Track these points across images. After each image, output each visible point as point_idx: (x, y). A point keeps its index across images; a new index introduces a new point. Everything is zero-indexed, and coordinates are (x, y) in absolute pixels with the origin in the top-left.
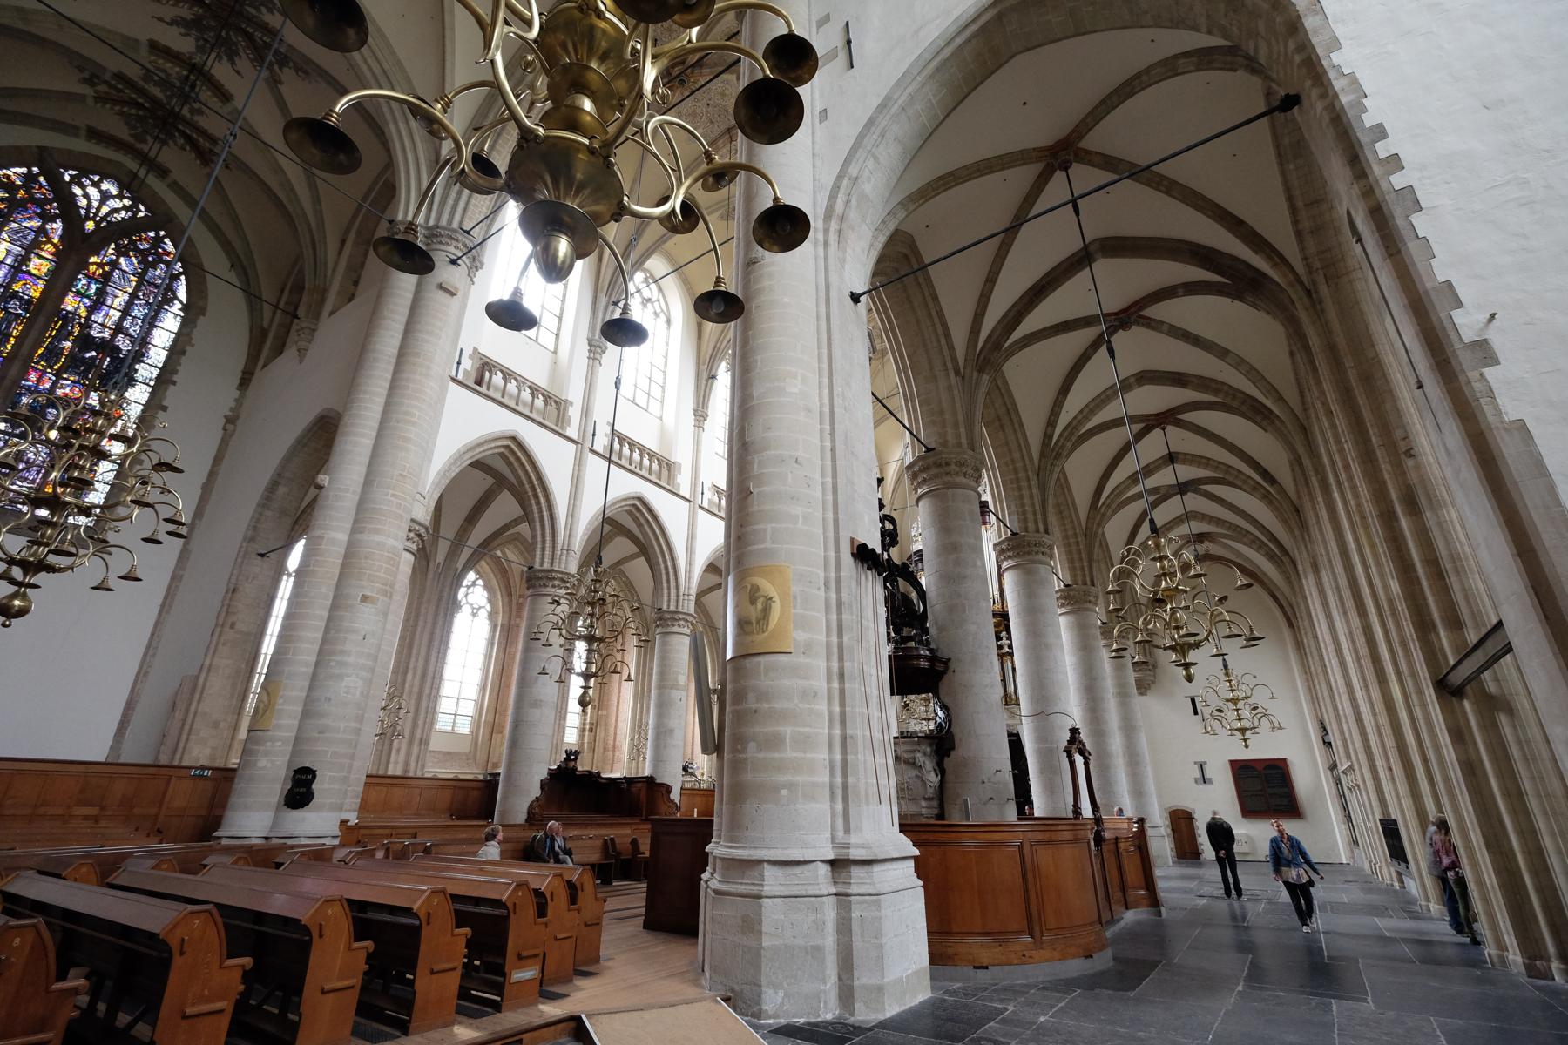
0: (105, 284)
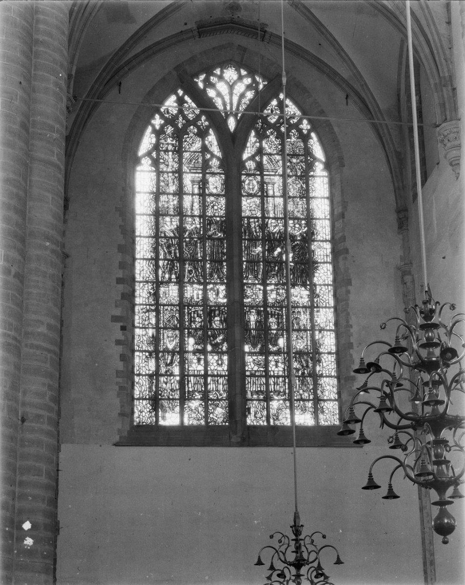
0: (262, 175)
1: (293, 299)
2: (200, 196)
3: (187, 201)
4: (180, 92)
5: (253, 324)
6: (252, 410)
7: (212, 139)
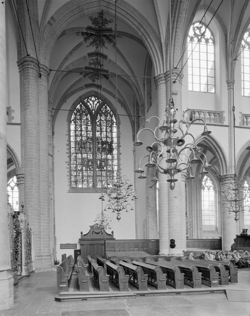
0: (101, 126)
1: (108, 158)
2: (86, 131)
3: (83, 133)
4: (81, 103)
5: (98, 164)
6: (98, 184)
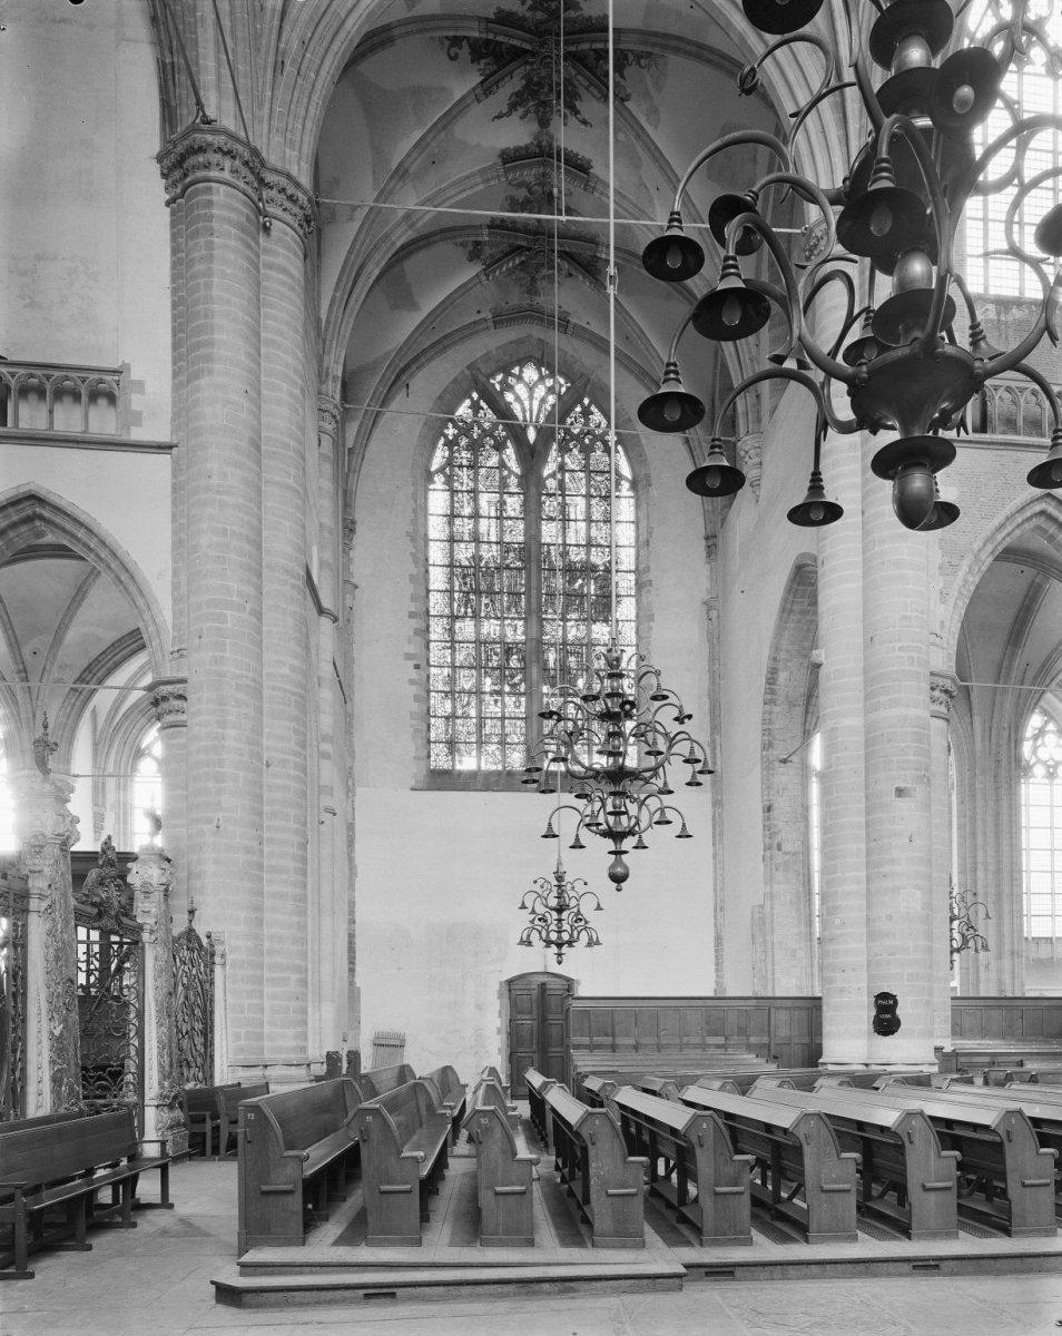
1: (594, 636)
2: (496, 519)
3: (483, 523)
4: (475, 396)
5: (551, 664)
7: (510, 451)
